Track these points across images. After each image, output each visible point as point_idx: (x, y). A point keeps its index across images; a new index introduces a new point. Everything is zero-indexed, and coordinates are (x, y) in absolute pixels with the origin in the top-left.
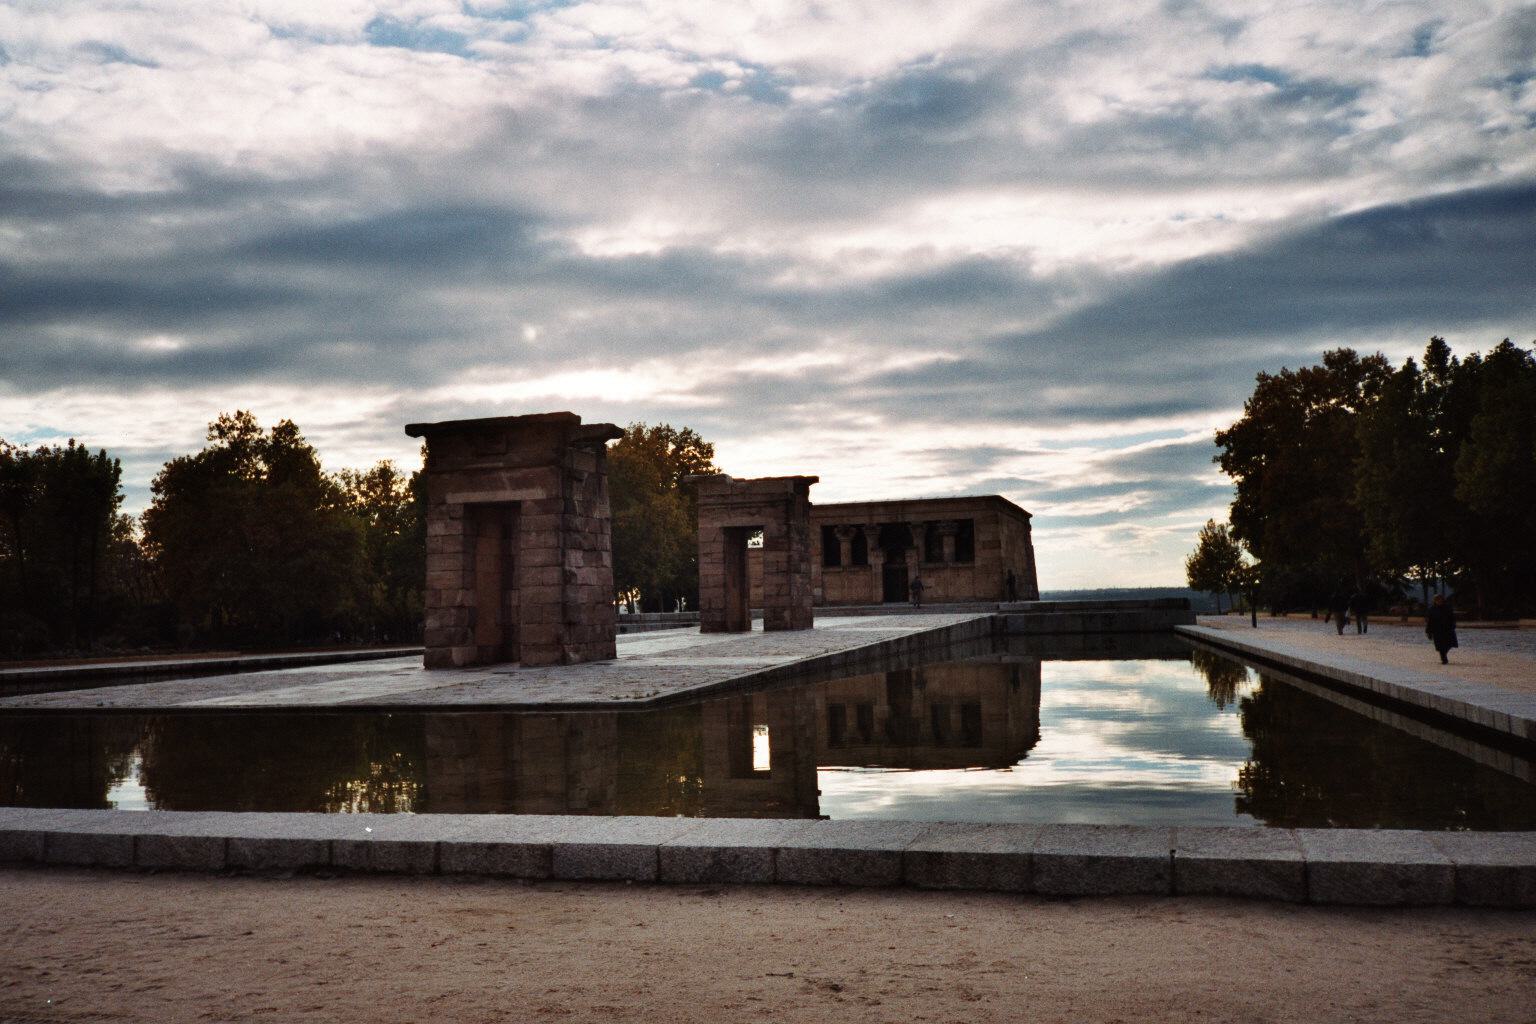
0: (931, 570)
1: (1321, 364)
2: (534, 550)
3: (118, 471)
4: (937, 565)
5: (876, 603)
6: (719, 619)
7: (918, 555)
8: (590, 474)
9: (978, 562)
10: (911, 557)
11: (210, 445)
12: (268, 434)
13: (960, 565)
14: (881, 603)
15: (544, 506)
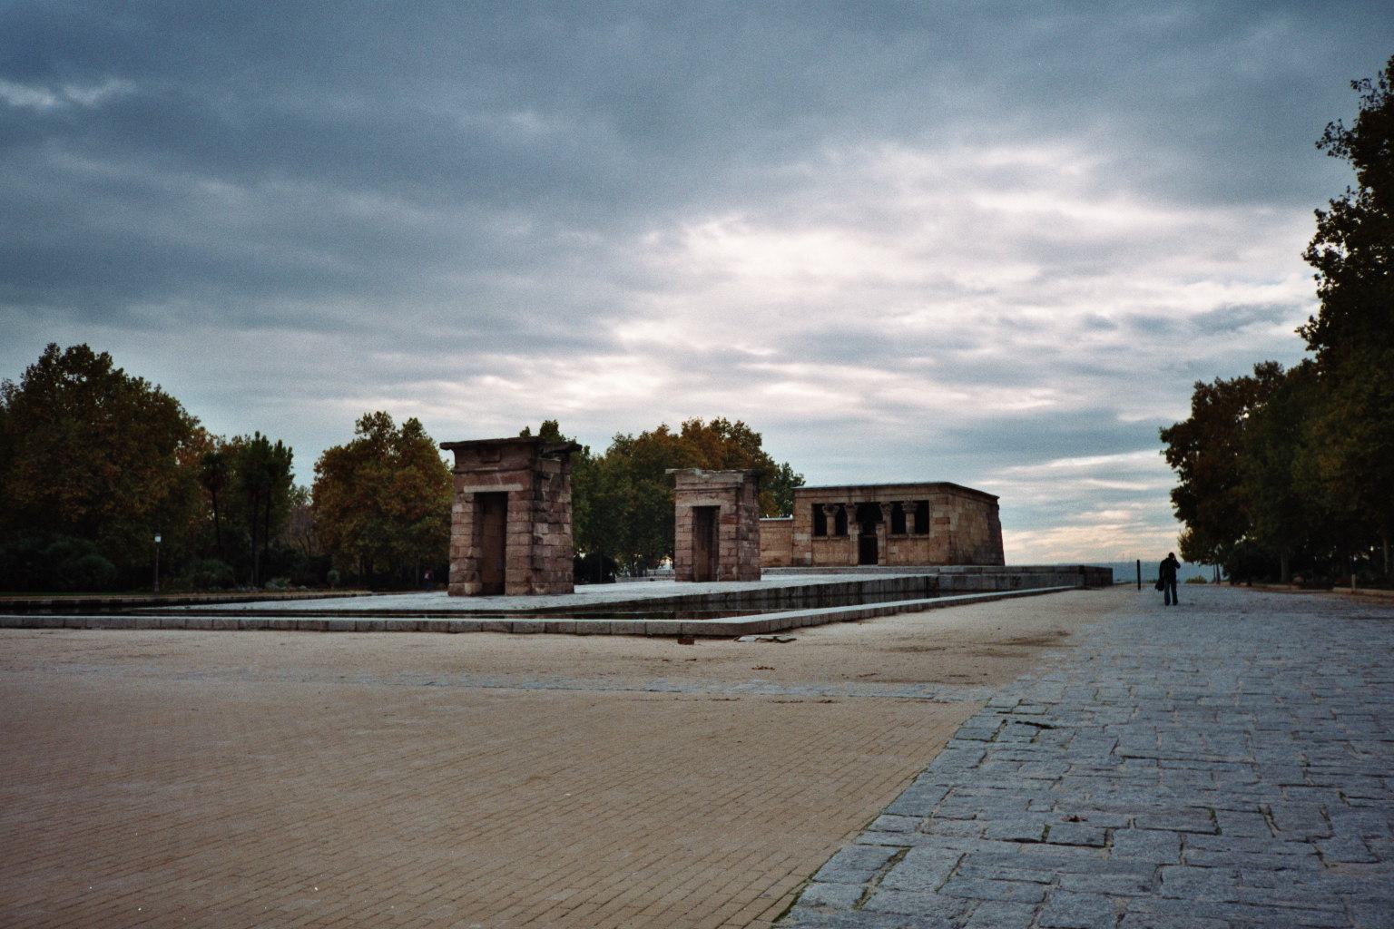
0: (895, 540)
1: (1253, 376)
2: (516, 524)
3: (291, 456)
4: (901, 536)
5: (853, 565)
6: (687, 572)
7: (885, 527)
8: (556, 475)
9: (932, 535)
10: (880, 529)
11: (356, 437)
12: (399, 427)
13: (918, 537)
14: (857, 565)
15: (521, 495)
